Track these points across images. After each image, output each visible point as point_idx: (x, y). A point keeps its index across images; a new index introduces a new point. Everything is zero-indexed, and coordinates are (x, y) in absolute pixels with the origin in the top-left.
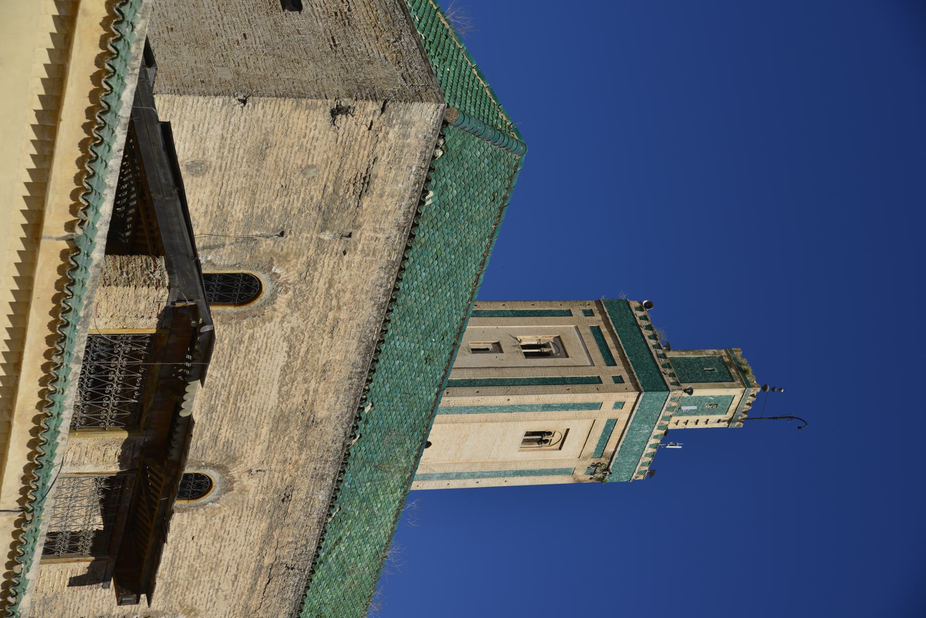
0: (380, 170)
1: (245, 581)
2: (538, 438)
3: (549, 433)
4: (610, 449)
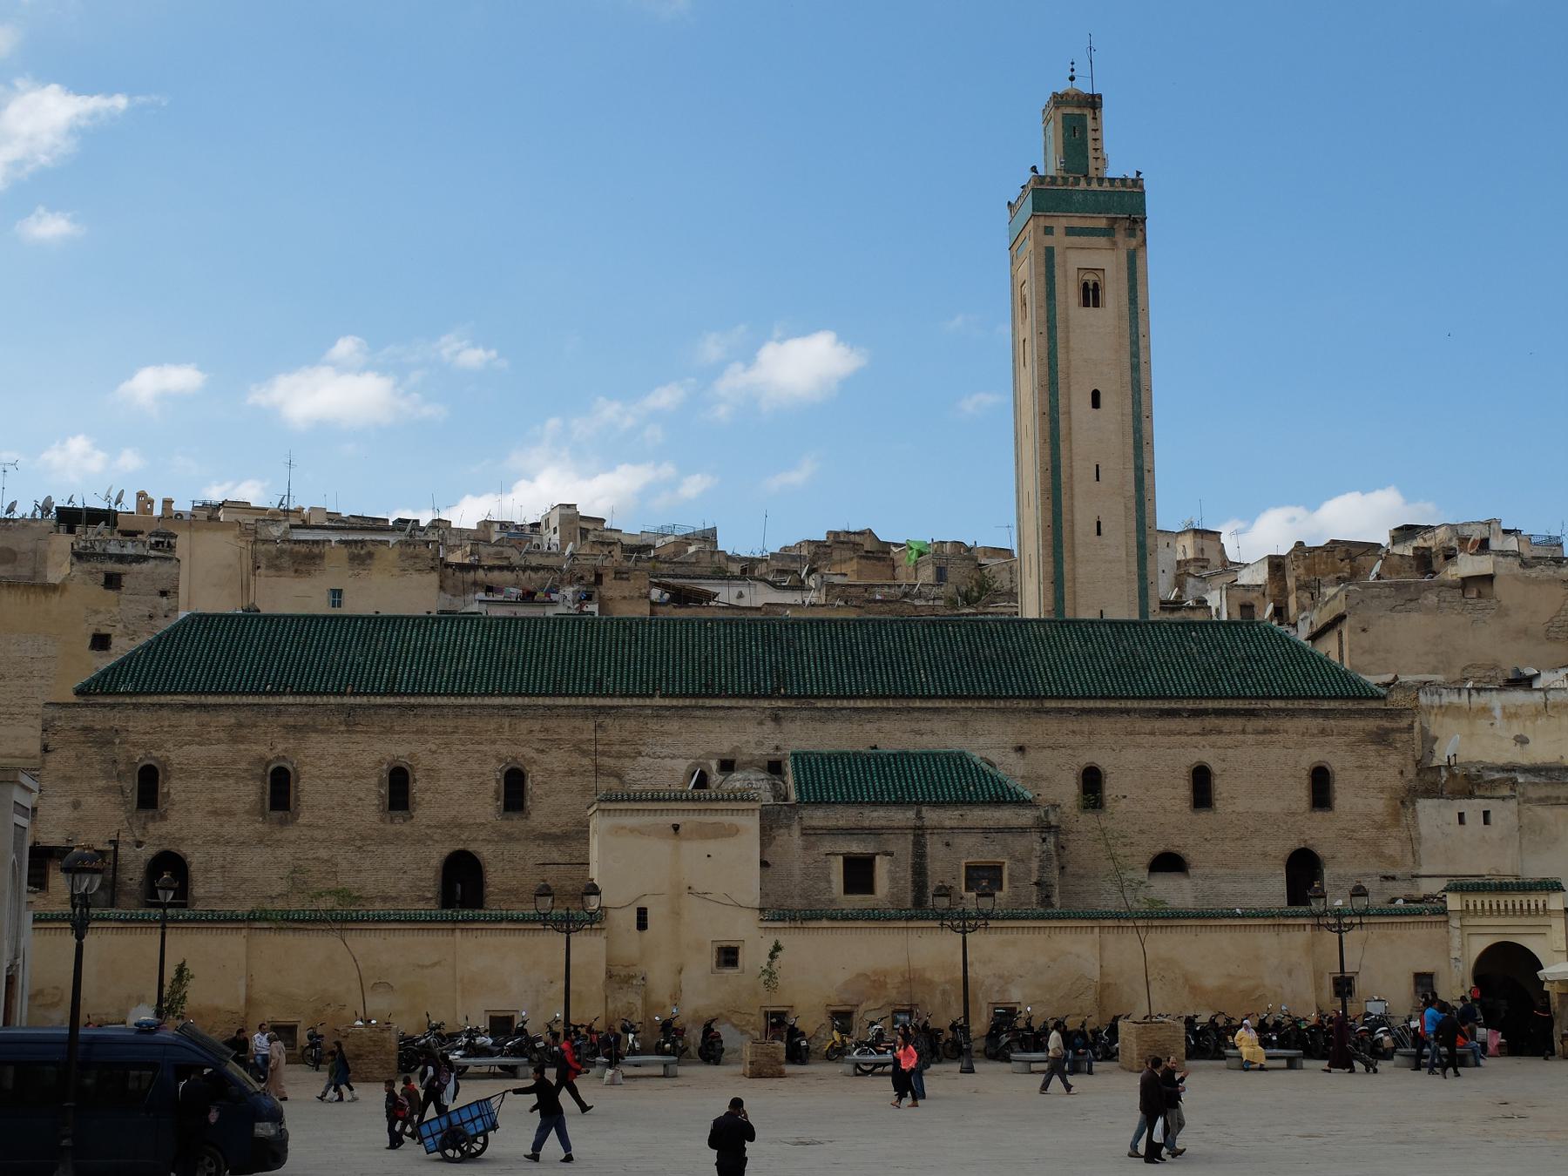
0: (79, 725)
1: (358, 737)
2: (1091, 295)
3: (1086, 285)
4: (1102, 223)
